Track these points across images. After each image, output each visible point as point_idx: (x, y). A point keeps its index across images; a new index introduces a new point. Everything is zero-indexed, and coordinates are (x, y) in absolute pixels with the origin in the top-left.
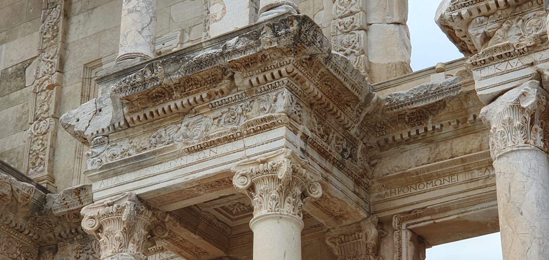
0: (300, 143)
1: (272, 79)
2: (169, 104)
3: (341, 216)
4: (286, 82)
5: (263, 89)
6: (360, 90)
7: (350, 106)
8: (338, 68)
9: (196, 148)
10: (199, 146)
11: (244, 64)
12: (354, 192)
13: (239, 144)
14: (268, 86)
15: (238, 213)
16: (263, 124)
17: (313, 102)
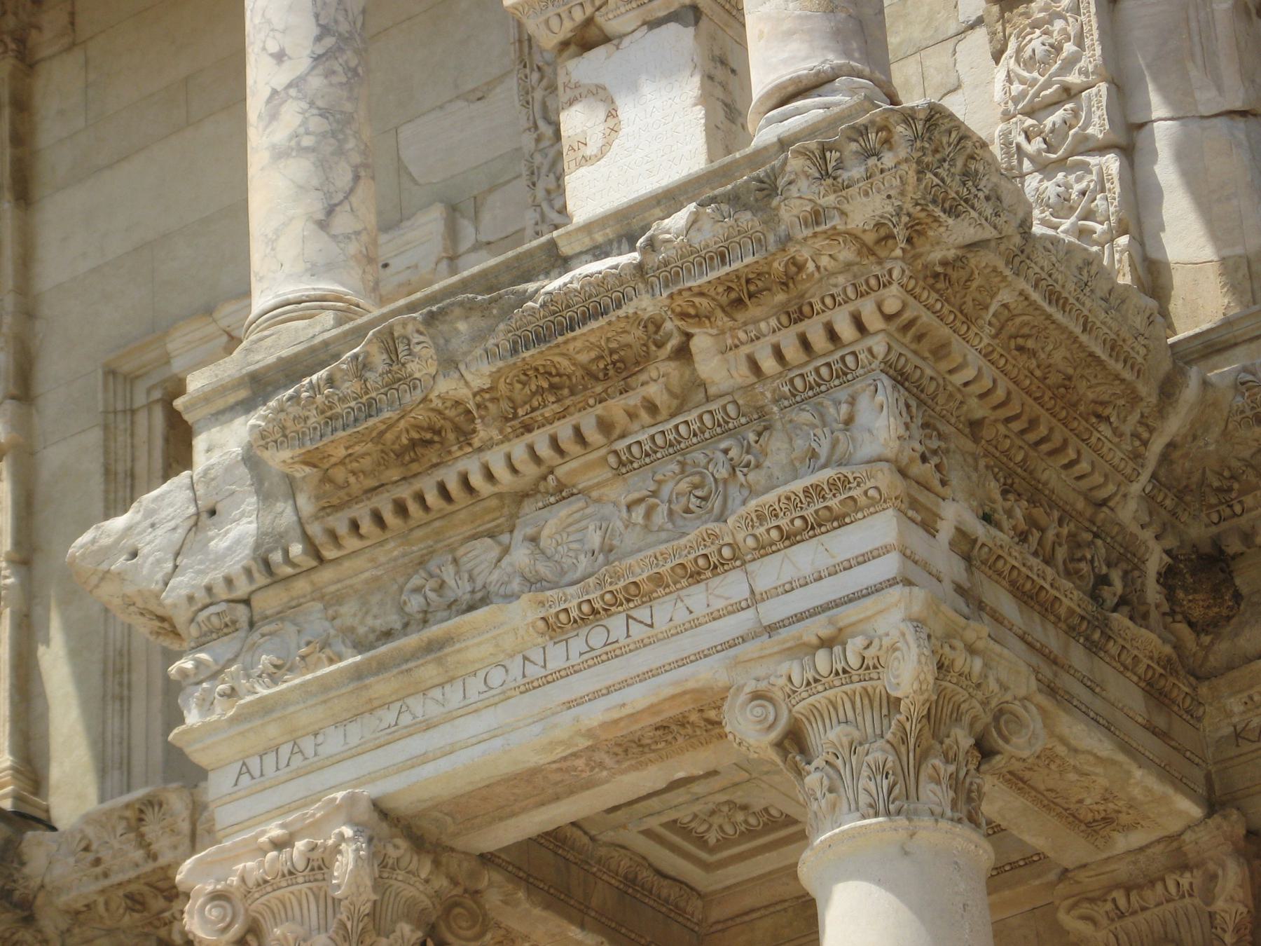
0: (951, 567)
1: (831, 347)
2: (461, 465)
3: (1107, 820)
4: (880, 348)
5: (799, 383)
6: (1140, 360)
7: (1108, 419)
8: (1058, 288)
9: (574, 613)
10: (585, 608)
11: (724, 300)
12: (1155, 731)
13: (732, 586)
14: (817, 370)
15: (724, 843)
16: (812, 510)
17: (978, 414)
